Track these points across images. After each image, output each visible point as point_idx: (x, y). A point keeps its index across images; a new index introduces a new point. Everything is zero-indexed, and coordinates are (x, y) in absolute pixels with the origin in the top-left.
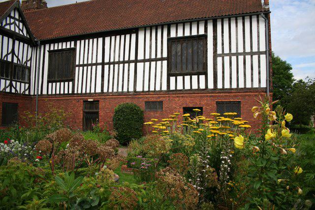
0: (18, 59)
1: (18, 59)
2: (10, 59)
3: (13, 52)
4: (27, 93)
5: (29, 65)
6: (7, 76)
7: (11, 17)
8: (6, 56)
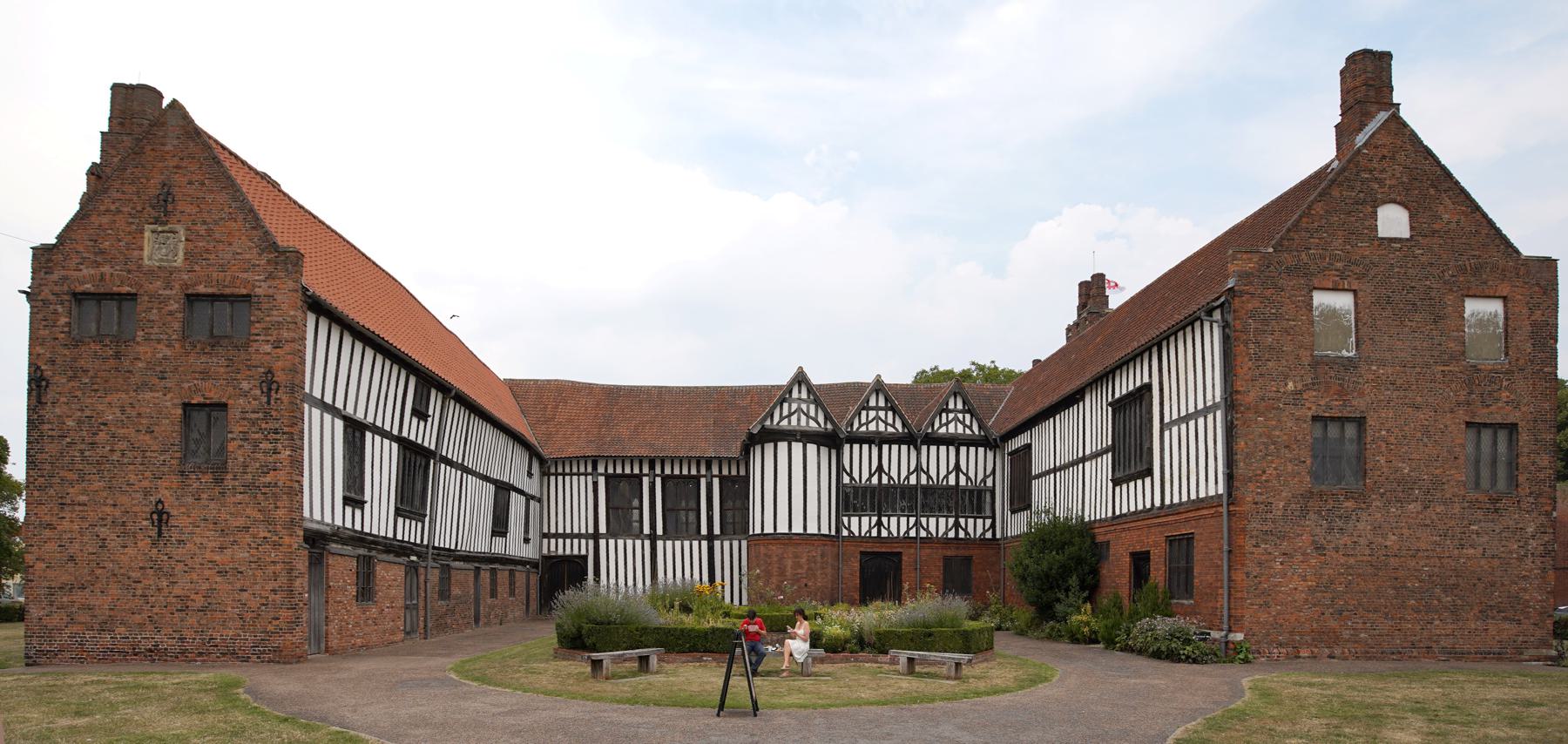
0: (968, 478)
1: (968, 478)
2: (952, 482)
3: (957, 467)
4: (989, 535)
5: (989, 483)
6: (949, 510)
7: (948, 411)
8: (946, 477)
